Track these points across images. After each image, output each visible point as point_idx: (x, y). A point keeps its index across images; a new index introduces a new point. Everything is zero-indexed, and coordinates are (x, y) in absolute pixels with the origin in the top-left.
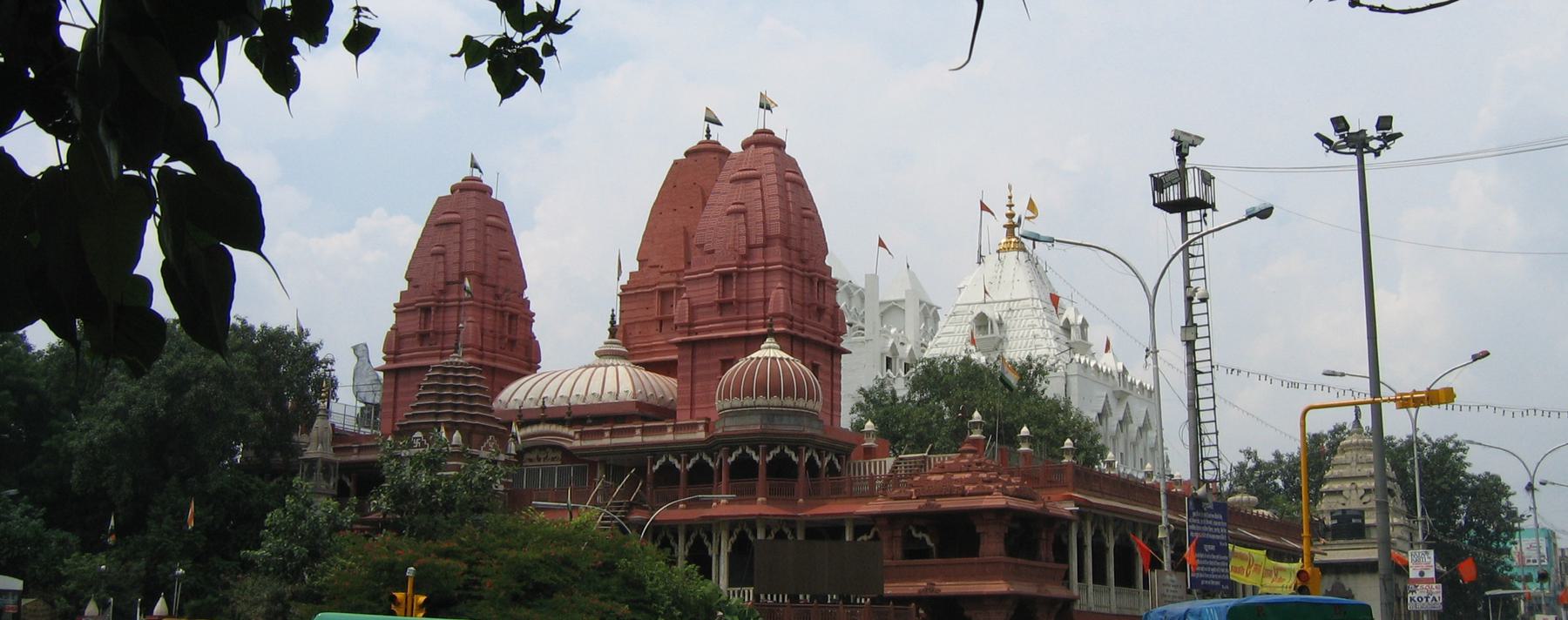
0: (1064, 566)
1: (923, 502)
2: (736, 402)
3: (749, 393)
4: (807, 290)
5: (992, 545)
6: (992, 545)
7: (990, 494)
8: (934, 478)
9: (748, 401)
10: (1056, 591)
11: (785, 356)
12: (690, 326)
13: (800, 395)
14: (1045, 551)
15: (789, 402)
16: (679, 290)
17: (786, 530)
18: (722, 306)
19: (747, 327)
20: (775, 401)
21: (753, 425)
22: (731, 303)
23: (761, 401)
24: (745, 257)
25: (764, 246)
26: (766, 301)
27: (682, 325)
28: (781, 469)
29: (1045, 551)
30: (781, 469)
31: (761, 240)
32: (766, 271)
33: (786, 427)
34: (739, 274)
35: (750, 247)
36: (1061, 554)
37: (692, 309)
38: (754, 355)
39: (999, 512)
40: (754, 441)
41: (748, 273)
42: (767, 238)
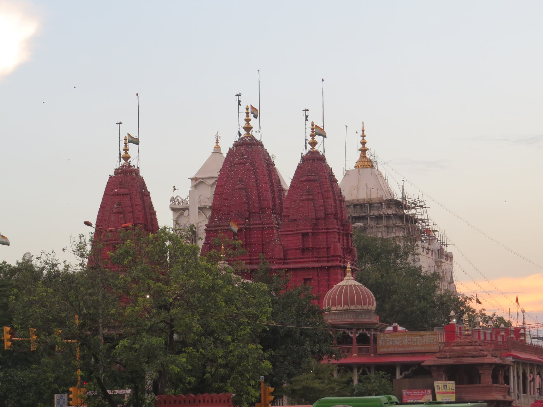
0: (508, 386)
1: (456, 359)
2: (339, 308)
3: (346, 303)
4: (345, 241)
5: (487, 378)
6: (487, 378)
7: (486, 356)
8: (456, 348)
9: (346, 308)
10: (508, 398)
11: (357, 283)
12: (285, 260)
13: (365, 303)
14: (501, 379)
15: (365, 307)
16: (246, 228)
17: (366, 369)
18: (304, 250)
19: (317, 262)
20: (359, 307)
21: (349, 319)
22: (308, 249)
23: (352, 307)
24: (315, 225)
25: (325, 219)
26: (328, 248)
27: (278, 259)
28: (363, 339)
29: (501, 379)
30: (363, 339)
31: (323, 216)
32: (327, 232)
33: (365, 320)
34: (313, 233)
35: (317, 219)
36: (507, 380)
37: (284, 251)
38: (341, 283)
39: (491, 365)
40: (350, 327)
41: (318, 233)
42: (326, 214)
